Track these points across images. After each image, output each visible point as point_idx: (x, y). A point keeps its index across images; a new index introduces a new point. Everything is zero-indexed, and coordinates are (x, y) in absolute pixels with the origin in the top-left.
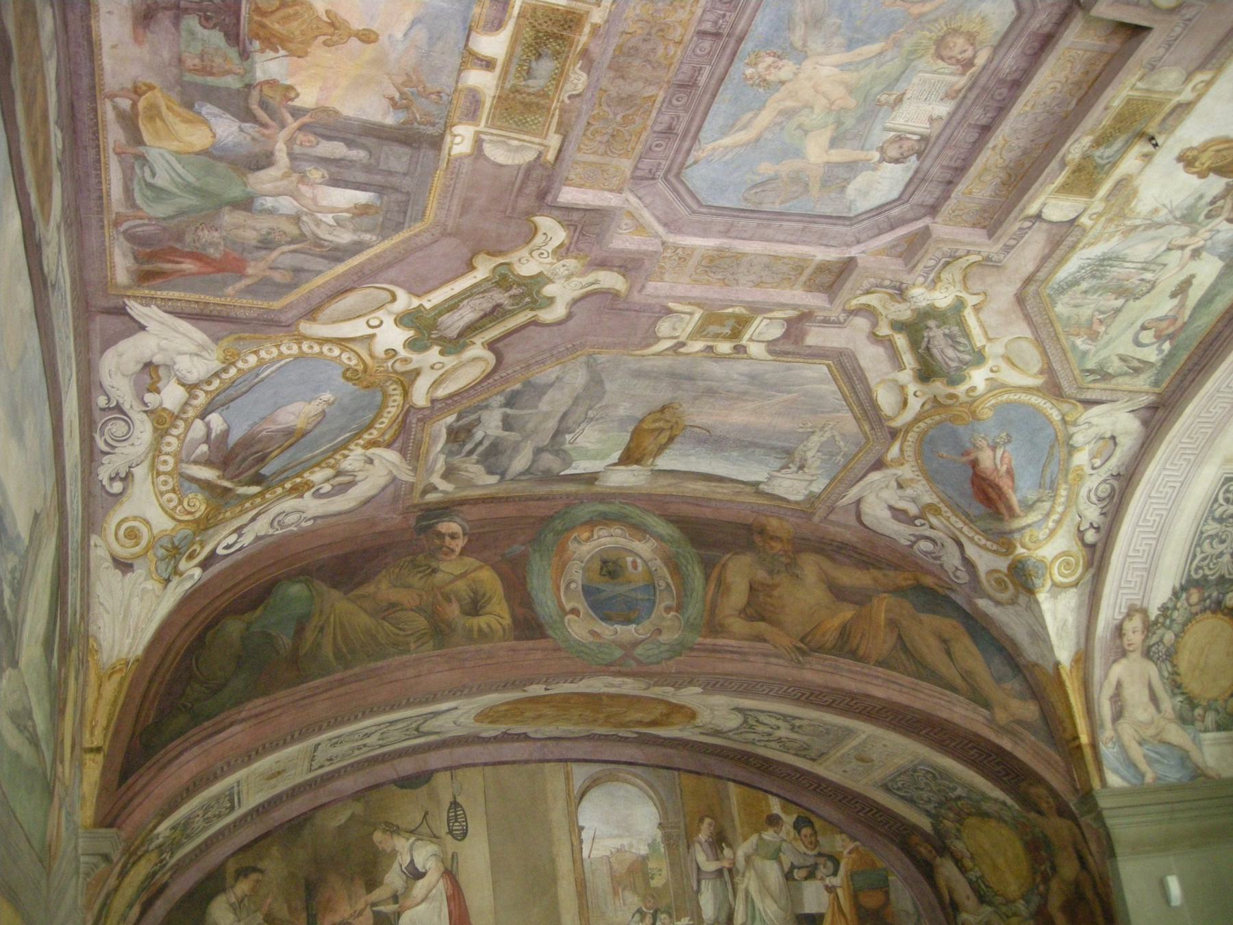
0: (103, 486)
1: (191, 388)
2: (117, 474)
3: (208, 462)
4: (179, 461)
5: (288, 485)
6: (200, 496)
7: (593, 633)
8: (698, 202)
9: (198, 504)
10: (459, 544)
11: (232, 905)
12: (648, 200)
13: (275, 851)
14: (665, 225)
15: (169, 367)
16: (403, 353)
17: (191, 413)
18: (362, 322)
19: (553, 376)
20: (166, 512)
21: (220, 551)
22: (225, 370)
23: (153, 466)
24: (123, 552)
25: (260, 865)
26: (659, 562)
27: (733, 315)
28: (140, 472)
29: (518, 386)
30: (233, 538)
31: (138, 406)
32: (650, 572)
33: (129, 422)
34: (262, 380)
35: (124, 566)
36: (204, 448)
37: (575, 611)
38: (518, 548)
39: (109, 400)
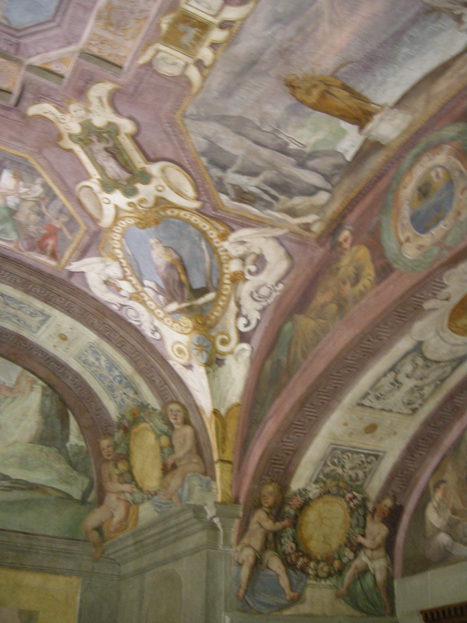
0: (154, 339)
1: (125, 278)
2: (153, 330)
3: (169, 301)
4: (162, 309)
5: (227, 281)
6: (184, 318)
7: (420, 247)
8: (49, 22)
9: (187, 322)
10: (349, 241)
11: (435, 508)
12: (40, 49)
13: (450, 467)
14: (70, 44)
15: (110, 278)
16: (134, 200)
17: (139, 287)
18: (105, 206)
19: (201, 140)
20: (180, 333)
21: (243, 329)
22: (121, 263)
23: (158, 318)
24: (184, 361)
25: (445, 478)
26: (453, 159)
27: (173, 25)
28: (157, 323)
29: (204, 160)
30: (242, 321)
31: (125, 300)
32: (448, 172)
33: (131, 308)
34: (133, 255)
35: (189, 367)
36: (161, 297)
37: (408, 240)
38: (375, 220)
39: (116, 305)
